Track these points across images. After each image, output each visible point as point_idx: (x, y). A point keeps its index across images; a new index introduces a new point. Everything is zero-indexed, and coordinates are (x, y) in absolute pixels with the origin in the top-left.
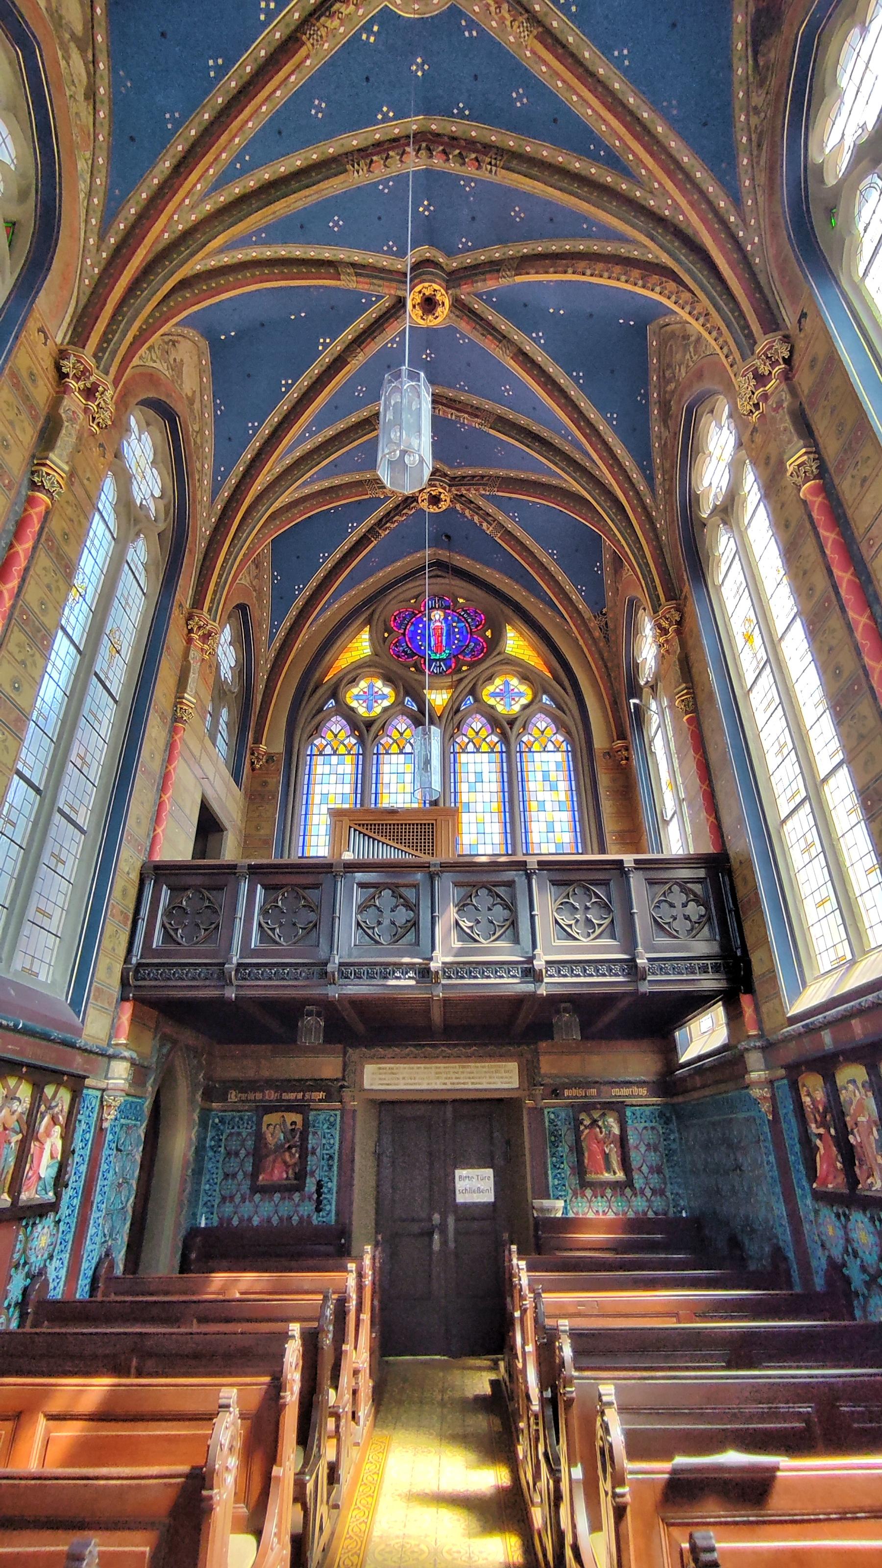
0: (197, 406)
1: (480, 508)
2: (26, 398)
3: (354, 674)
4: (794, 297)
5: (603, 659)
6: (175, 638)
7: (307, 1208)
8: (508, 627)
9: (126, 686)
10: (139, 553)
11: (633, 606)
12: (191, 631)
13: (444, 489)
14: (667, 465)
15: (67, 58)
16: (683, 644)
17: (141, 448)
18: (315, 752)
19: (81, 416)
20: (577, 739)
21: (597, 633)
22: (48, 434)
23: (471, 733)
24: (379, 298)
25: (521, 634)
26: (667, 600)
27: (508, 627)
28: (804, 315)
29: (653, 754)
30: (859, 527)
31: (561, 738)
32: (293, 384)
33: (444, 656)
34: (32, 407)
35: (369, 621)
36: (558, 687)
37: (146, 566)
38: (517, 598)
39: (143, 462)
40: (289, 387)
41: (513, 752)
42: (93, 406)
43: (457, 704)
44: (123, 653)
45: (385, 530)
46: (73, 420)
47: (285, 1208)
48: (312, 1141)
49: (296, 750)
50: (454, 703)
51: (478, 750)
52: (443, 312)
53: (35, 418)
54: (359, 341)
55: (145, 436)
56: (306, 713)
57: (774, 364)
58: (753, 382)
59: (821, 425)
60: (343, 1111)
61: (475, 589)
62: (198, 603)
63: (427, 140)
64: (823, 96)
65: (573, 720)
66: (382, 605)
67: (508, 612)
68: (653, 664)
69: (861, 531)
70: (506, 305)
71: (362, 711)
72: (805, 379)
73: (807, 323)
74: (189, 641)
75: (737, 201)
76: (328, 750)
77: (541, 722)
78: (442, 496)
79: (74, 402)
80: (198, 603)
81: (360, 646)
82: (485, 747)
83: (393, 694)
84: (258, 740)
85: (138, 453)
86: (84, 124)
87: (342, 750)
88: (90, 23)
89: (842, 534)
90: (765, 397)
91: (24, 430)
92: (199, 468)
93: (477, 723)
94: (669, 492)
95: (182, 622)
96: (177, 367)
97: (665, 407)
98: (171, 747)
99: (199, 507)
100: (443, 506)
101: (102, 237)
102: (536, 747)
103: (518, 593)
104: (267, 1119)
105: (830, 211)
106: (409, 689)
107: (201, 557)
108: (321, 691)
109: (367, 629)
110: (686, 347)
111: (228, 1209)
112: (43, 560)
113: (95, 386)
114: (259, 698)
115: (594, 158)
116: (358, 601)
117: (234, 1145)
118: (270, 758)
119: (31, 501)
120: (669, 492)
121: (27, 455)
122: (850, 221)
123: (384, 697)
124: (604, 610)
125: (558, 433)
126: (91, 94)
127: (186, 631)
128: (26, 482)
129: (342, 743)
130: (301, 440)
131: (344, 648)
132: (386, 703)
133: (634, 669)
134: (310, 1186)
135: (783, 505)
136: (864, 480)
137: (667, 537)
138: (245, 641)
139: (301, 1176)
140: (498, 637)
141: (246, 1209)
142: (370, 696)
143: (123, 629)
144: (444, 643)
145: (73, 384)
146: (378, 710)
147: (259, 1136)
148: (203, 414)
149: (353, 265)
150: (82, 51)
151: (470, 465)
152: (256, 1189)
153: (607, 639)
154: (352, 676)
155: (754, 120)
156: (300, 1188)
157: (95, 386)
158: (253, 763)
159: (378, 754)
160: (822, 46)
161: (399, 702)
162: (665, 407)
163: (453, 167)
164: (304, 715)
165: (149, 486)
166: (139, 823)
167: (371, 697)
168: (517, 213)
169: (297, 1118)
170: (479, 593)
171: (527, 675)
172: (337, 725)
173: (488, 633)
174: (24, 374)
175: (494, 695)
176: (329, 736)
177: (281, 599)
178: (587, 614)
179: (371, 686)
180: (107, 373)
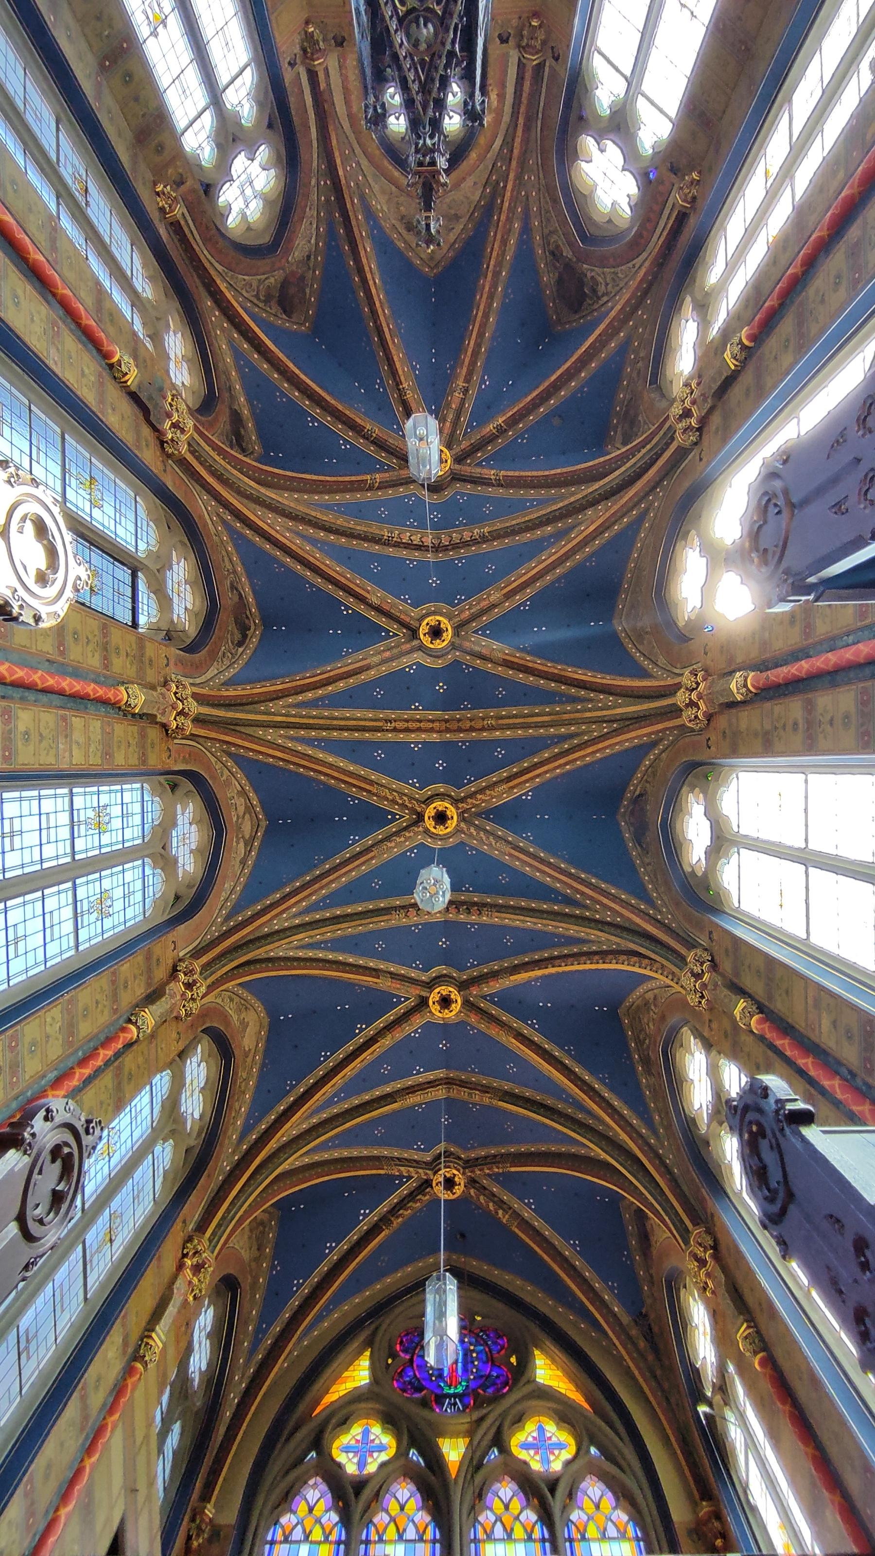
0: (249, 1060)
1: (494, 1195)
2: (149, 970)
3: (344, 1412)
4: (701, 929)
5: (655, 1377)
6: (169, 1250)
8: (537, 1352)
9: (102, 1286)
10: (165, 1154)
11: (673, 1285)
12: (185, 1256)
13: (458, 1170)
14: (660, 1105)
15: (238, 843)
16: (725, 1269)
17: (198, 1070)
18: (279, 1536)
19: (178, 997)
20: (645, 1510)
21: (642, 1344)
22: (152, 998)
23: (498, 1505)
24: (407, 999)
25: (553, 1361)
26: (694, 1225)
27: (537, 1352)
28: (711, 933)
29: (754, 1509)
30: (800, 1024)
31: (625, 1517)
32: (358, 841)
33: (460, 1389)
34: (150, 978)
35: (369, 1343)
36: (608, 1430)
37: (165, 1172)
38: (543, 1309)
39: (195, 1083)
40: (327, 1058)
41: (560, 1541)
42: (189, 994)
43: (478, 1454)
44: (116, 1245)
45: (398, 1217)
46: (172, 996)
49: (254, 1523)
50: (474, 1452)
51: (509, 1536)
52: (456, 1007)
53: (149, 985)
54: (389, 1027)
55: (203, 1064)
56: (276, 1469)
57: (702, 964)
58: (693, 980)
59: (747, 982)
61: (495, 1302)
62: (201, 1228)
63: (449, 1082)
64: (681, 845)
65: (635, 1484)
66: (388, 1321)
67: (536, 1330)
68: (714, 1360)
69: (803, 1025)
70: (504, 1000)
71: (351, 1469)
72: (726, 966)
73: (715, 936)
74: (181, 1266)
75: (650, 902)
76: (298, 1534)
77: (593, 1489)
78: (456, 1179)
79: (178, 987)
80: (201, 1228)
81: (359, 1374)
82: (519, 1532)
83: (394, 1444)
84: (205, 1497)
85: (195, 1073)
86: (238, 859)
87: (317, 1534)
88: (253, 838)
89: (793, 1038)
90: (704, 986)
91: (139, 985)
92: (237, 1108)
93: (506, 1490)
94: (668, 1127)
95: (180, 1241)
96: (244, 1025)
97: (646, 1061)
98: (119, 1390)
99: (227, 1141)
100: (459, 1190)
101: (228, 918)
102: (592, 1531)
103: (546, 1304)
105: (708, 888)
106: (416, 1436)
107: (216, 1189)
109: (368, 1353)
110: (649, 1009)
112: (107, 1080)
113: (195, 982)
114: (222, 1430)
115: (555, 901)
116: (362, 1311)
118: (216, 1533)
119: (123, 1030)
120: (668, 1127)
121: (134, 1002)
122: (719, 885)
123: (382, 1448)
124: (644, 1311)
125: (560, 1098)
126: (243, 862)
127: (180, 1255)
128: (125, 1017)
129: (318, 1521)
130: (329, 1103)
131: (337, 1378)
132: (384, 1457)
133: (694, 1375)
135: (749, 1055)
136: (787, 992)
137: (679, 1169)
138: (224, 1337)
140: (525, 1364)
142: (364, 1447)
143: (125, 1220)
144: (460, 1372)
145: (182, 976)
146: (372, 1468)
148: (252, 1068)
149: (391, 973)
150: (246, 845)
151: (483, 1145)
153: (656, 1350)
154: (343, 1416)
155: (649, 868)
157: (195, 982)
158: (189, 1538)
159: (367, 1542)
160: (672, 827)
161: (401, 1453)
162: (646, 1061)
163: (462, 917)
164: (275, 1467)
165: (194, 1106)
166: (47, 1477)
167: (365, 1448)
168: (509, 940)
170: (499, 1306)
171: (565, 1414)
172: (315, 1494)
173: (513, 1360)
174: (155, 958)
175: (526, 1446)
176: (302, 1508)
177: (276, 1294)
178: (626, 1319)
179: (366, 1433)
180: (205, 979)
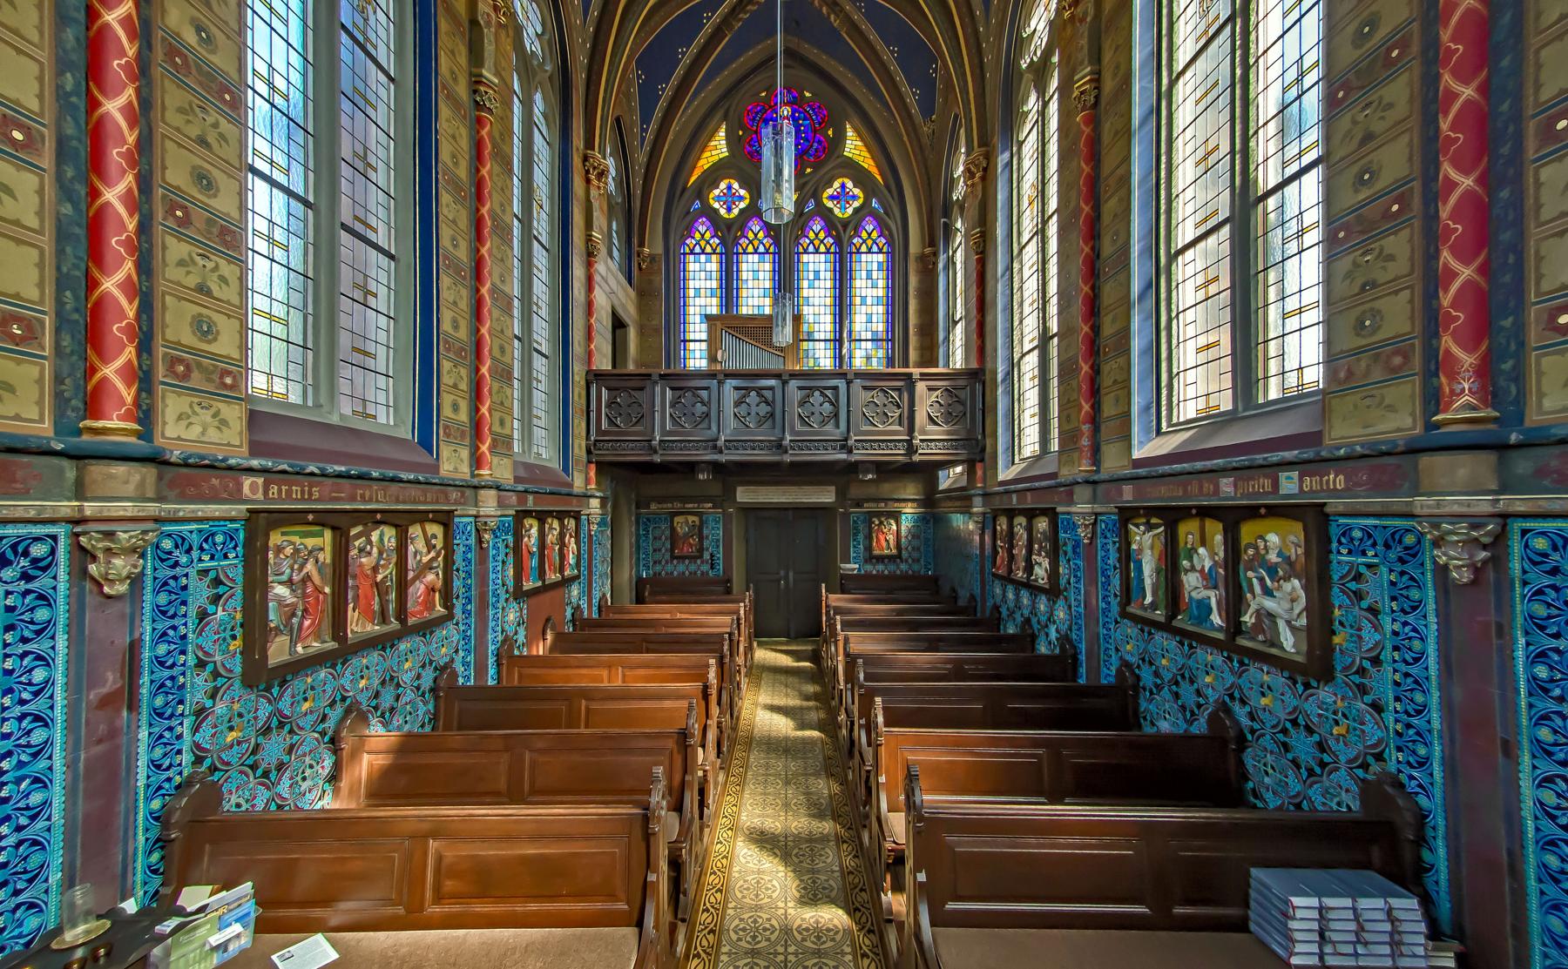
7: (705, 568)
47: (693, 567)
48: (705, 532)
60: (724, 513)
76: (697, 250)
87: (708, 249)
104: (677, 519)
108: (686, 195)
111: (658, 568)
117: (658, 533)
134: (707, 556)
139: (701, 550)
141: (669, 568)
147: (673, 529)
152: (673, 557)
156: (701, 557)
169: (696, 519)
172: (702, 227)
176: (698, 236)
